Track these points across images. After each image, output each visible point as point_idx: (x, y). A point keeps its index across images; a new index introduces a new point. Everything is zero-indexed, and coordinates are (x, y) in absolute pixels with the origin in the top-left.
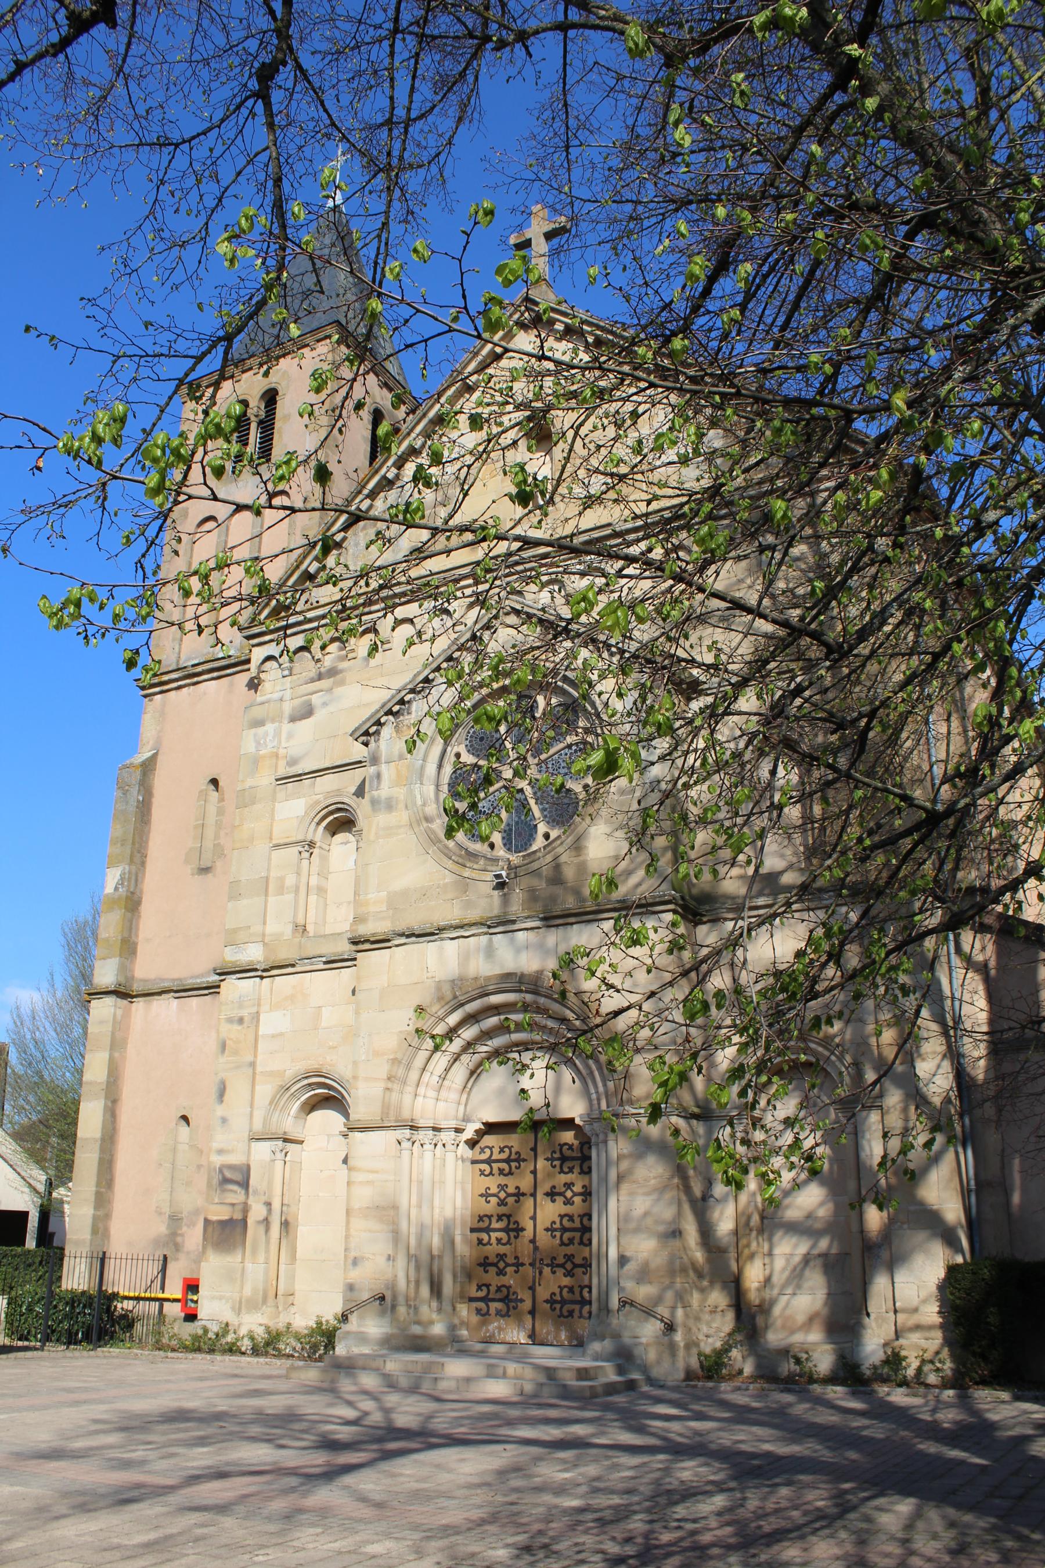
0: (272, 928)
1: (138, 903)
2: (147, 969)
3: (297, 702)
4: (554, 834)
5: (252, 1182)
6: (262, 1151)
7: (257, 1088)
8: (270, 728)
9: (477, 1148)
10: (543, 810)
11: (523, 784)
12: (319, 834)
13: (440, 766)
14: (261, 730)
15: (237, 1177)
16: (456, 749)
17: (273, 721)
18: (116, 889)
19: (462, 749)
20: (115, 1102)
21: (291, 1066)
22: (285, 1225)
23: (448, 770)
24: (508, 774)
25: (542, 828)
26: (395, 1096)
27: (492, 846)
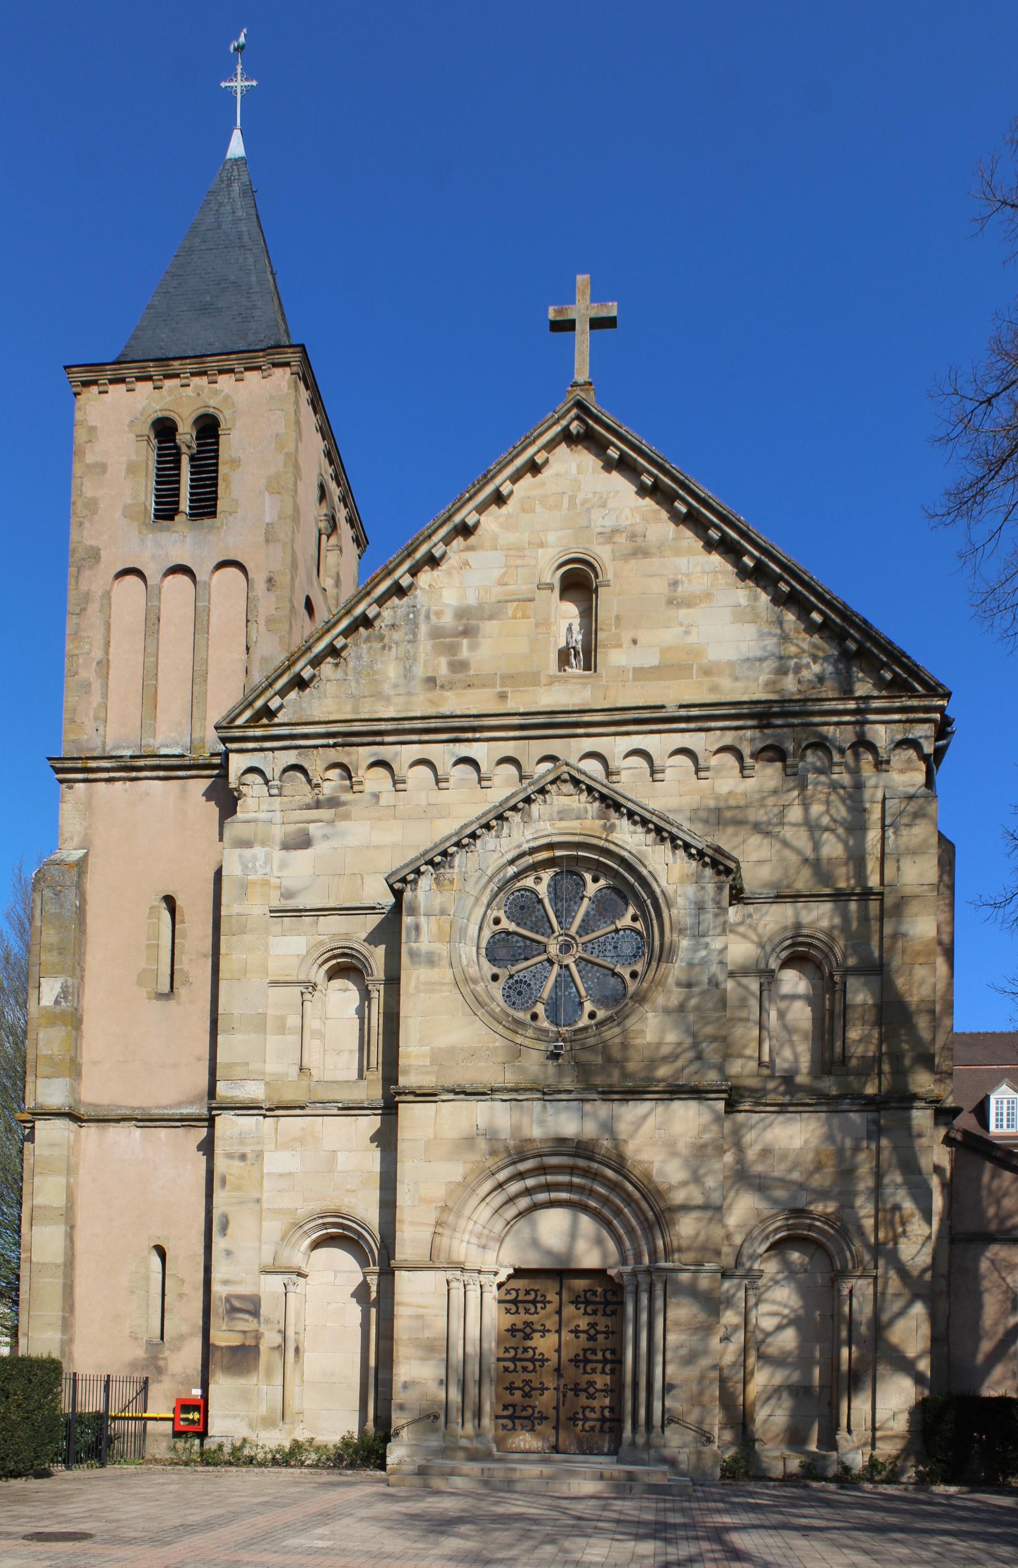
0: (272, 1067)
1: (80, 1021)
2: (96, 1091)
3: (291, 828)
4: (601, 1014)
5: (263, 1311)
6: (273, 1284)
7: (264, 1223)
8: (258, 851)
9: (503, 1289)
10: (587, 990)
11: (570, 961)
12: (319, 976)
13: (481, 929)
14: (247, 852)
15: (250, 1307)
16: (493, 914)
17: (263, 844)
18: (57, 1002)
19: (501, 914)
20: (72, 1227)
21: (305, 1206)
22: (297, 1350)
23: (487, 934)
24: (553, 949)
25: (588, 1007)
26: (445, 1241)
27: (535, 1017)
